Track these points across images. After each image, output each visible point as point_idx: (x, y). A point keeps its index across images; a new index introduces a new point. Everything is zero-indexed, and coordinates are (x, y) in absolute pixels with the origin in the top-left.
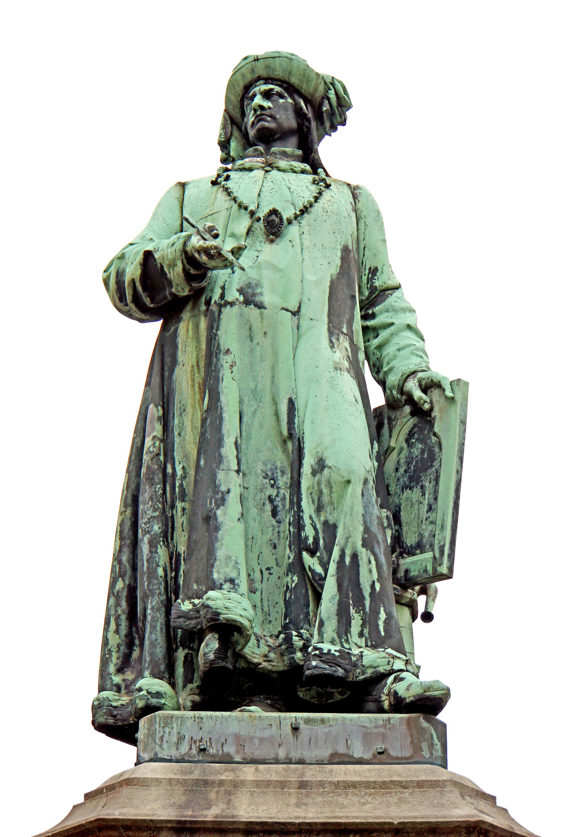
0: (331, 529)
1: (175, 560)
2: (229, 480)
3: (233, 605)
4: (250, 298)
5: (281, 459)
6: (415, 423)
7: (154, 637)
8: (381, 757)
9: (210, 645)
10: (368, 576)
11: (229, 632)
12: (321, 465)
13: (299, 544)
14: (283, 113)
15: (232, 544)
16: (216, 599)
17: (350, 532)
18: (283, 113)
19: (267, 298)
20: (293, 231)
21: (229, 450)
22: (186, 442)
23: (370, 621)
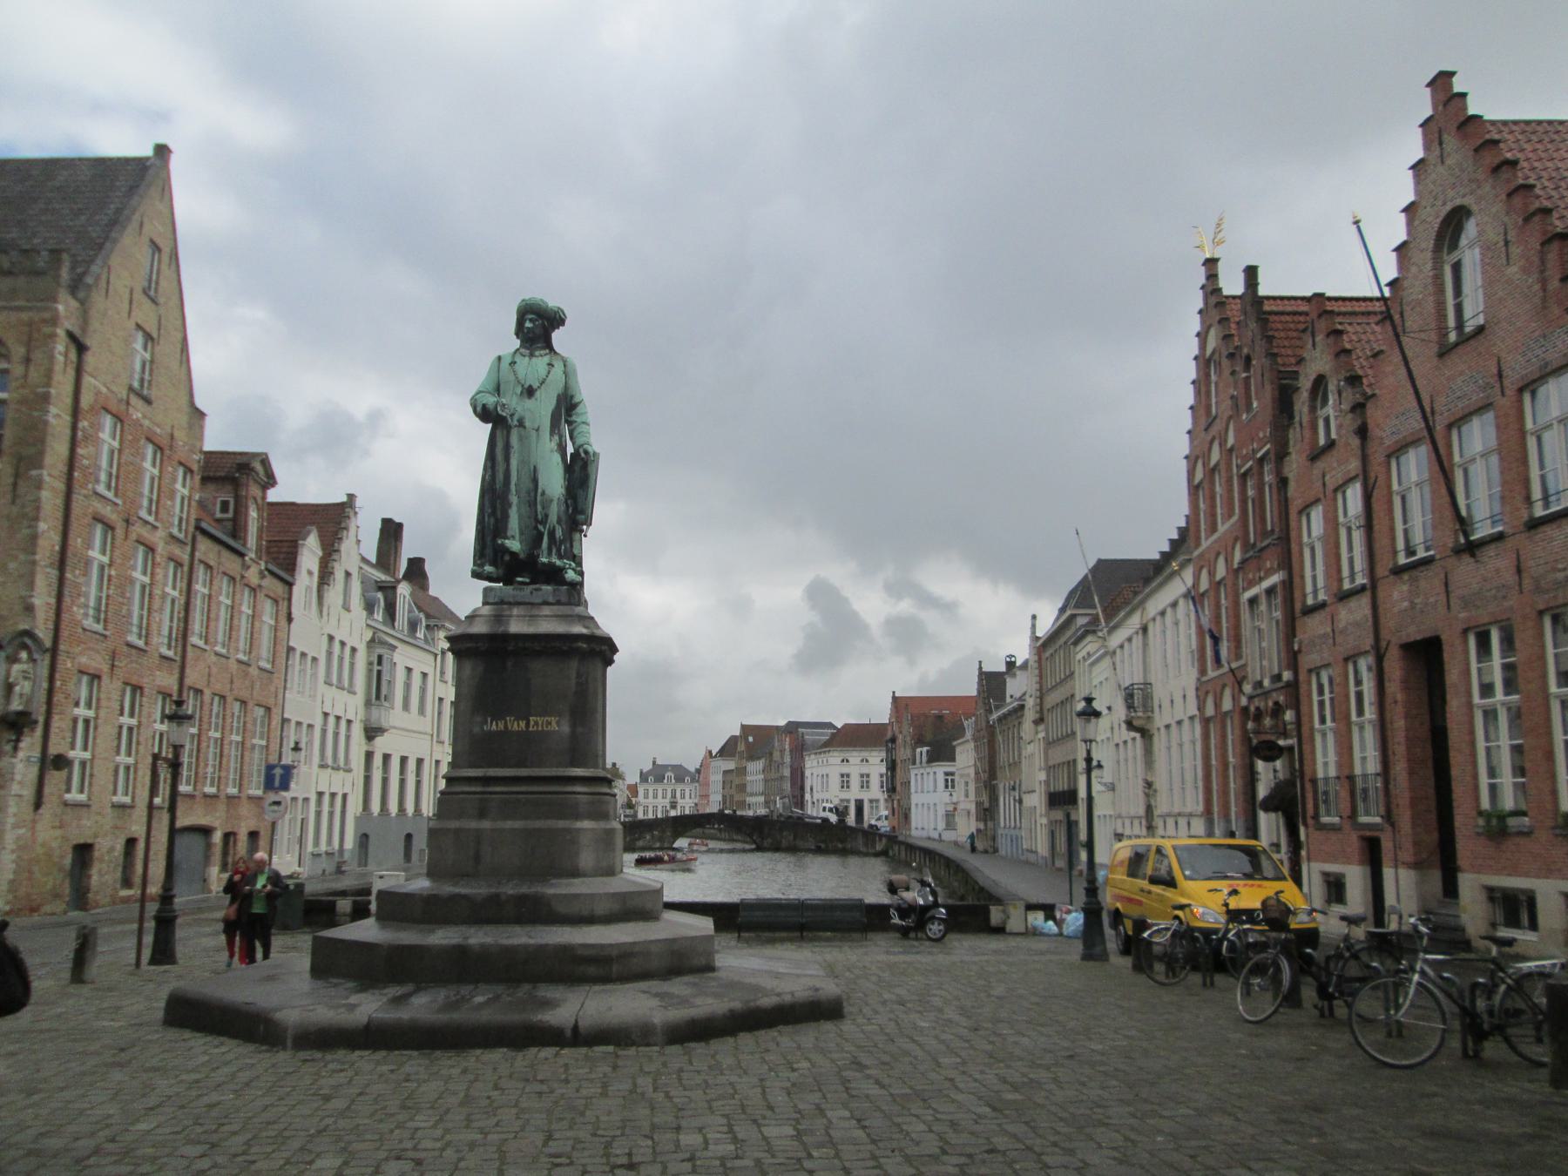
0: (547, 516)
1: (497, 520)
2: (514, 499)
3: (514, 545)
4: (521, 424)
5: (531, 486)
6: (580, 471)
7: (489, 551)
8: (558, 603)
9: (507, 558)
10: (559, 533)
11: (513, 554)
12: (543, 493)
13: (537, 521)
14: (538, 325)
15: (514, 523)
16: (508, 543)
17: (553, 518)
18: (538, 325)
19: (527, 424)
20: (538, 394)
21: (513, 487)
22: (500, 476)
23: (559, 550)
